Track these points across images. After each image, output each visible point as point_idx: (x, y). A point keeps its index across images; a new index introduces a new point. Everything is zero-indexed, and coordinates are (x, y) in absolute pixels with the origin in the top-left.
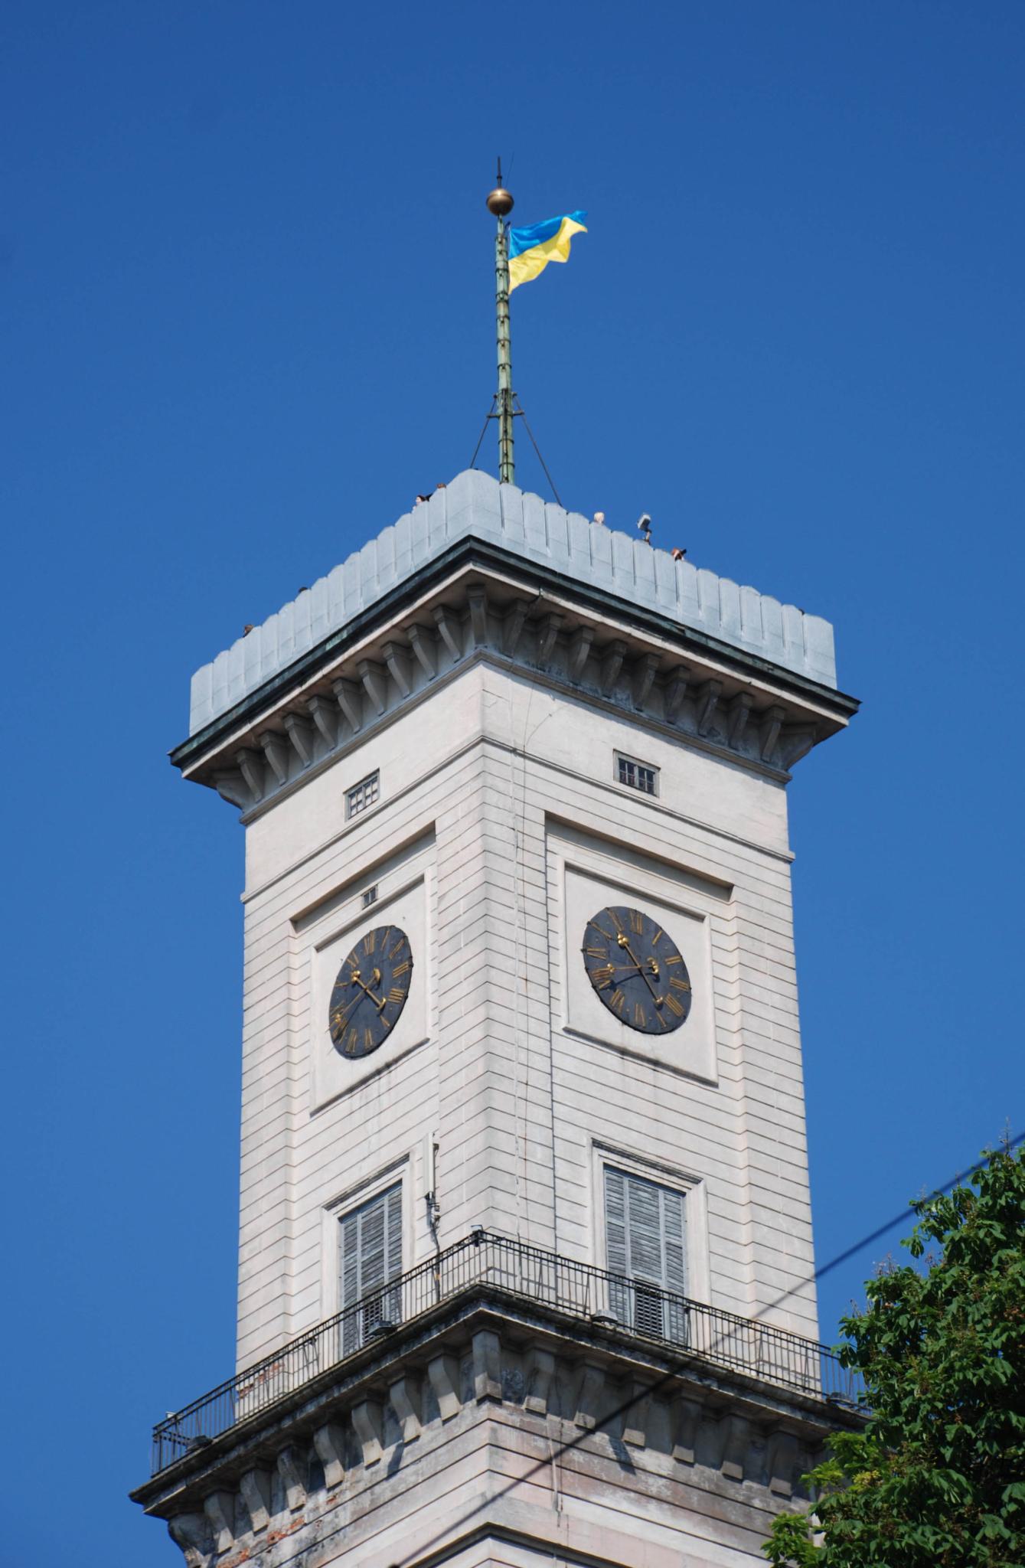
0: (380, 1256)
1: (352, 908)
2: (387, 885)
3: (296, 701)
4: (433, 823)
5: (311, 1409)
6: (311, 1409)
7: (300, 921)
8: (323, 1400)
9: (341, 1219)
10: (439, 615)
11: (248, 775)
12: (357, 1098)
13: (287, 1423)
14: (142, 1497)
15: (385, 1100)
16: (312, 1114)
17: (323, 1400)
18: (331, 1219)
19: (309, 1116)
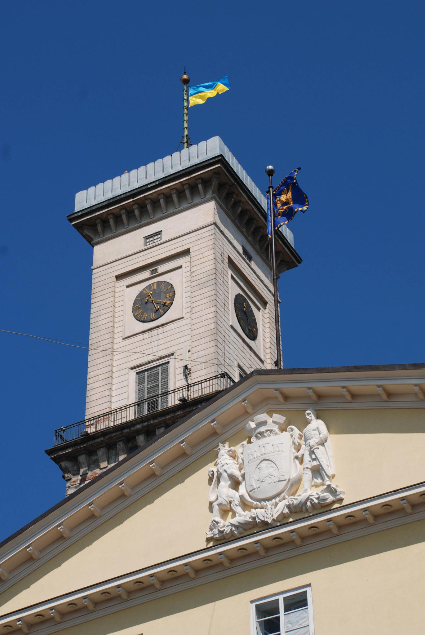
0: (158, 385)
1: (146, 274)
2: (162, 268)
3: (129, 204)
4: (189, 248)
5: (139, 426)
6: (139, 426)
7: (119, 277)
8: (146, 424)
9: (137, 373)
10: (200, 181)
11: (99, 228)
12: (146, 335)
13: (126, 430)
14: (49, 452)
15: (161, 336)
16: (123, 339)
17: (146, 424)
18: (133, 373)
19: (122, 339)
